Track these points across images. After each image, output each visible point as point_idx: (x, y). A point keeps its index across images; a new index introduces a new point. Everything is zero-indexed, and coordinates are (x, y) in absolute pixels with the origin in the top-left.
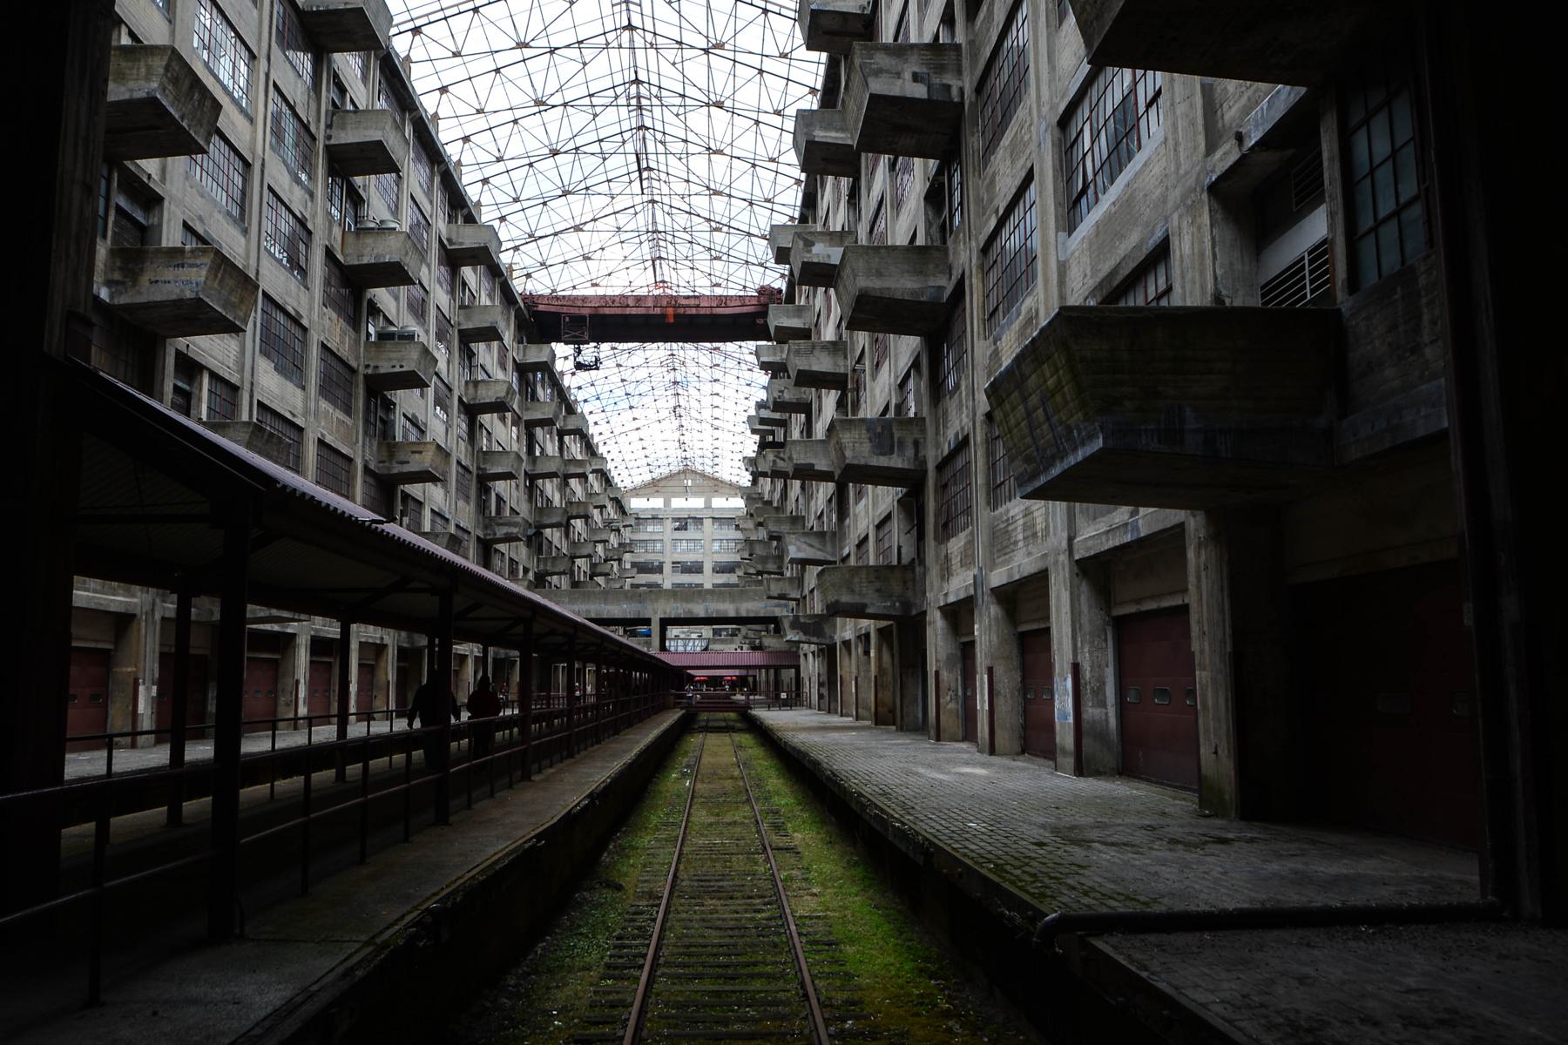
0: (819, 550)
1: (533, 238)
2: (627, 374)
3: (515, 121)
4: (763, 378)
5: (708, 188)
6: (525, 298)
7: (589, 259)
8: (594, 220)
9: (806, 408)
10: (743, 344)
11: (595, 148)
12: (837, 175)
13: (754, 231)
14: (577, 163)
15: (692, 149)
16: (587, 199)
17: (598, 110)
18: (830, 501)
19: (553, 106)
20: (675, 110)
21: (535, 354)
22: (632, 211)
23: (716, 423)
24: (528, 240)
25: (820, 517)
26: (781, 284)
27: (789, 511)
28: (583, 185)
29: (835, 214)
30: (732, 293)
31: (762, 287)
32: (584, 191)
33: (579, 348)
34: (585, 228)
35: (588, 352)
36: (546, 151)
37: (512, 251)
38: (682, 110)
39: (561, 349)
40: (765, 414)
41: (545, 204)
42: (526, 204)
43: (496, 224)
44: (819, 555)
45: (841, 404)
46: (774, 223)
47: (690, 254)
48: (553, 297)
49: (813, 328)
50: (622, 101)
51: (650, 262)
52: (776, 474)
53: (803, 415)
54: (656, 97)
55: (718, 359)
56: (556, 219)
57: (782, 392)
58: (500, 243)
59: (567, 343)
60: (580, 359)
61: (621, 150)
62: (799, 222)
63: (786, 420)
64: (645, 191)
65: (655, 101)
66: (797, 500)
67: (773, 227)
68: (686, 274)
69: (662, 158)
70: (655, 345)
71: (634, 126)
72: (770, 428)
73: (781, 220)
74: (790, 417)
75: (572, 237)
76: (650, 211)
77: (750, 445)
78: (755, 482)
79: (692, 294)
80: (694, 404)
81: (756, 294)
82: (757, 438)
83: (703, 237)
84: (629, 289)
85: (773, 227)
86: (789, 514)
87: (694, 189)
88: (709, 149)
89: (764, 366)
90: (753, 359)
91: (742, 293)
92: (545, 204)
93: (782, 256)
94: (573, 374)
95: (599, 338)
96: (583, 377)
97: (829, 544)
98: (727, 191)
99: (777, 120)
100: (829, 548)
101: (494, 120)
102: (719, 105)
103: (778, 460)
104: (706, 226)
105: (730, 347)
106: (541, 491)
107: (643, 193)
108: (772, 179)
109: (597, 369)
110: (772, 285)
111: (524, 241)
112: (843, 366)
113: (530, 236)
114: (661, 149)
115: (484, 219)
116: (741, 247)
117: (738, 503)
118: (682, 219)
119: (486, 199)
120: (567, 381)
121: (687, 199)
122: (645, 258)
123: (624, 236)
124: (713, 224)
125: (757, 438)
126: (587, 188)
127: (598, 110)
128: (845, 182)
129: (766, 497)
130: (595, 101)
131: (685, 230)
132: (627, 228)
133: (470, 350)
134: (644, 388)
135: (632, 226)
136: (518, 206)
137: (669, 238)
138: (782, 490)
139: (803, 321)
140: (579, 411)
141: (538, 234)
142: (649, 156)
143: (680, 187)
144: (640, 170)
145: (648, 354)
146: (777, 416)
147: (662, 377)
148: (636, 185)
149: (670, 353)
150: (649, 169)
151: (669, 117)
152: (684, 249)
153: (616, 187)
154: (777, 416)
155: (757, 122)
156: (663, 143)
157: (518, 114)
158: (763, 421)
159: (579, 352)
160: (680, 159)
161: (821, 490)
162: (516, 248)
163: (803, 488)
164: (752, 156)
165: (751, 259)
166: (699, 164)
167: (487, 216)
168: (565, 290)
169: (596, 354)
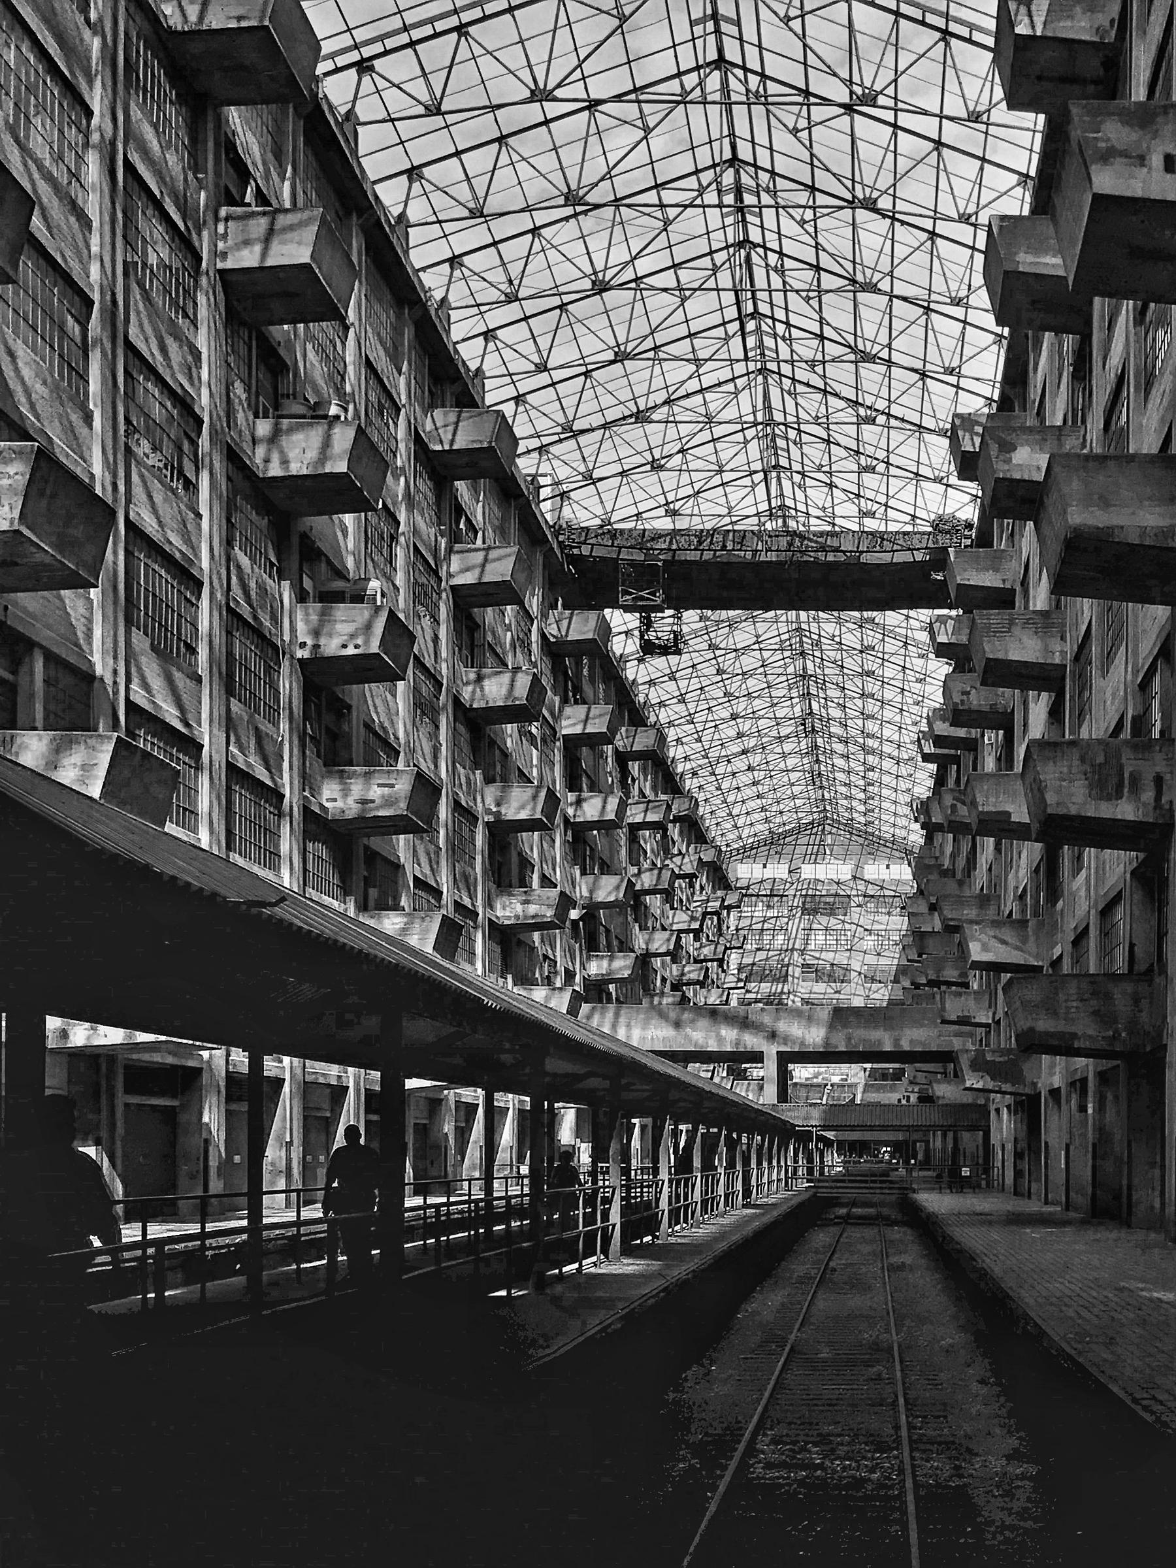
0: (1017, 948)
1: (570, 432)
2: (727, 662)
3: (535, 231)
4: (941, 669)
5: (853, 349)
6: (557, 530)
7: (661, 468)
8: (668, 402)
9: (1004, 721)
10: (912, 613)
11: (667, 279)
12: (1058, 330)
13: (928, 422)
14: (639, 306)
15: (828, 281)
16: (657, 369)
17: (672, 212)
18: (1037, 870)
19: (597, 206)
20: (797, 213)
21: (581, 627)
22: (730, 387)
23: (870, 742)
24: (562, 436)
25: (1022, 897)
26: (970, 513)
27: (978, 887)
28: (649, 343)
29: (1055, 394)
30: (893, 527)
31: (940, 518)
32: (651, 354)
33: (648, 618)
34: (655, 417)
35: (664, 624)
36: (587, 284)
37: (536, 455)
38: (809, 214)
39: (620, 620)
40: (942, 728)
41: (587, 374)
42: (557, 375)
43: (508, 409)
44: (1016, 957)
45: (1055, 714)
46: (960, 410)
47: (825, 462)
48: (607, 531)
49: (1018, 589)
50: (711, 197)
51: (761, 475)
52: (957, 828)
53: (1001, 732)
54: (767, 191)
55: (872, 637)
56: (607, 400)
57: (968, 693)
58: (515, 441)
59: (627, 609)
60: (651, 635)
61: (711, 284)
62: (998, 409)
63: (976, 740)
64: (750, 354)
65: (766, 199)
66: (990, 870)
67: (955, 415)
68: (818, 495)
69: (778, 298)
70: (771, 614)
71: (731, 241)
72: (953, 752)
73: (971, 405)
74: (983, 736)
75: (633, 432)
76: (760, 389)
77: (923, 781)
78: (929, 838)
79: (829, 528)
80: (836, 713)
81: (930, 529)
82: (933, 767)
83: (845, 434)
84: (727, 520)
85: (955, 415)
86: (978, 891)
87: (832, 350)
88: (853, 281)
89: (942, 651)
90: (924, 636)
91: (909, 528)
92: (587, 374)
93: (968, 466)
94: (641, 660)
95: (679, 604)
96: (658, 665)
97: (1032, 939)
98: (884, 354)
99: (964, 233)
100: (1031, 945)
101: (502, 228)
102: (870, 205)
103: (959, 805)
104: (849, 415)
105: (892, 618)
106: (592, 849)
107: (746, 359)
108: (957, 334)
109: (678, 652)
110: (958, 515)
111: (556, 438)
112: (1060, 652)
113: (564, 430)
114: (776, 281)
115: (489, 399)
116: (906, 450)
117: (902, 873)
118: (811, 403)
119: (491, 365)
120: (631, 672)
121: (819, 369)
122: (754, 466)
123: (718, 431)
124: (862, 411)
125: (933, 767)
126: (656, 348)
127: (672, 212)
128: (1069, 342)
129: (947, 864)
130: (668, 196)
131: (816, 421)
132: (721, 417)
133: (470, 617)
134: (753, 684)
135: (730, 413)
136: (544, 379)
137: (792, 434)
138: (969, 853)
139: (999, 576)
140: (653, 719)
141: (577, 426)
142: (759, 295)
143: (807, 349)
144: (741, 319)
145: (761, 627)
146: (961, 732)
147: (782, 666)
148: (736, 343)
149: (794, 626)
150: (756, 315)
151: (789, 227)
152: (815, 453)
153: (704, 347)
154: (961, 732)
155: (933, 235)
156: (781, 271)
157: (541, 218)
158: (939, 741)
159: (647, 624)
160: (807, 299)
161: (1024, 855)
162: (542, 449)
163: (998, 849)
164: (923, 294)
165: (924, 471)
166: (838, 312)
167: (495, 394)
168: (622, 516)
169: (675, 628)
